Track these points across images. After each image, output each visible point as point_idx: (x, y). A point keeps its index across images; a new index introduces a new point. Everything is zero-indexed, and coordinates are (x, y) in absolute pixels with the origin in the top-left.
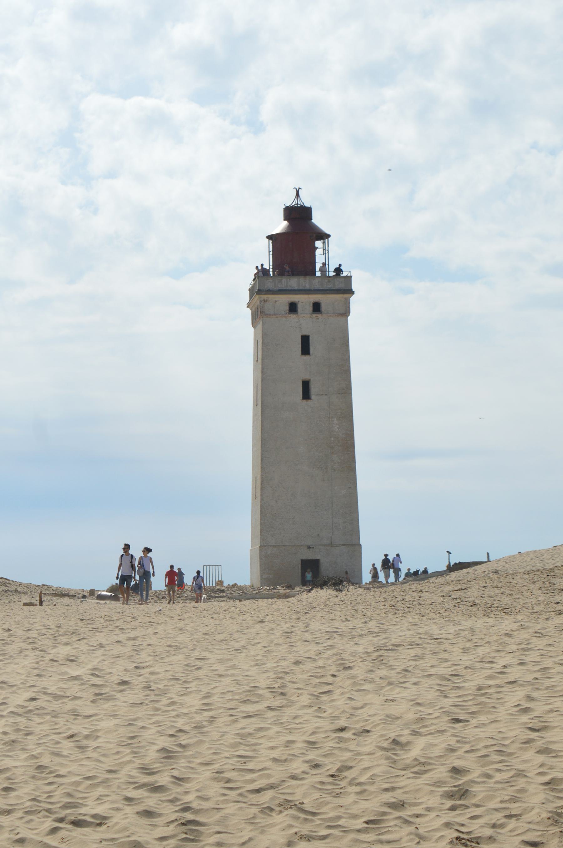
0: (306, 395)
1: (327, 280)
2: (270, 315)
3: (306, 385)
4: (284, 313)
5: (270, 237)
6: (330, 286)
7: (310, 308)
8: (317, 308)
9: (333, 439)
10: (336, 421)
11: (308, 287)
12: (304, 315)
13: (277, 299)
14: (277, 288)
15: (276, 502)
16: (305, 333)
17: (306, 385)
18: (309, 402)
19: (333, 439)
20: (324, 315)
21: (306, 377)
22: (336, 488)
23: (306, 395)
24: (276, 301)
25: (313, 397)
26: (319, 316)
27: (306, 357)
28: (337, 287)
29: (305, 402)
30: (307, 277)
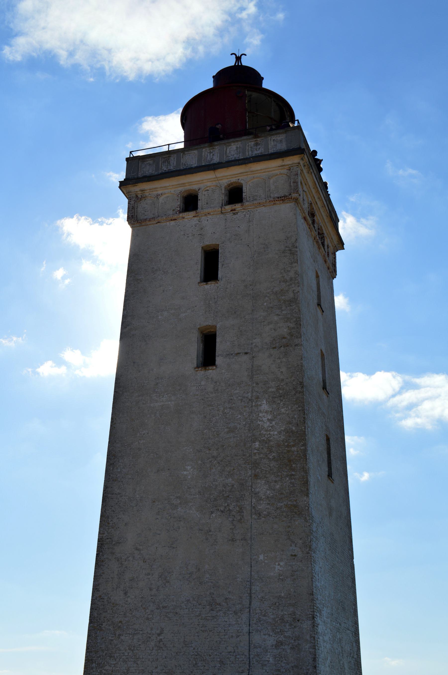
0: (208, 358)
1: (253, 143)
2: (146, 220)
3: (209, 341)
4: (171, 212)
5: (344, 249)
6: (259, 152)
7: (220, 196)
8: (235, 195)
9: (257, 444)
10: (265, 406)
11: (216, 159)
12: (210, 210)
13: (160, 192)
14: (160, 172)
15: (126, 594)
16: (209, 241)
17: (209, 341)
18: (211, 372)
19: (257, 444)
20: (247, 203)
21: (205, 321)
22: (261, 557)
23: (208, 358)
24: (158, 196)
25: (219, 360)
26: (238, 206)
27: (210, 286)
28: (271, 151)
29: (201, 373)
30: (216, 143)
